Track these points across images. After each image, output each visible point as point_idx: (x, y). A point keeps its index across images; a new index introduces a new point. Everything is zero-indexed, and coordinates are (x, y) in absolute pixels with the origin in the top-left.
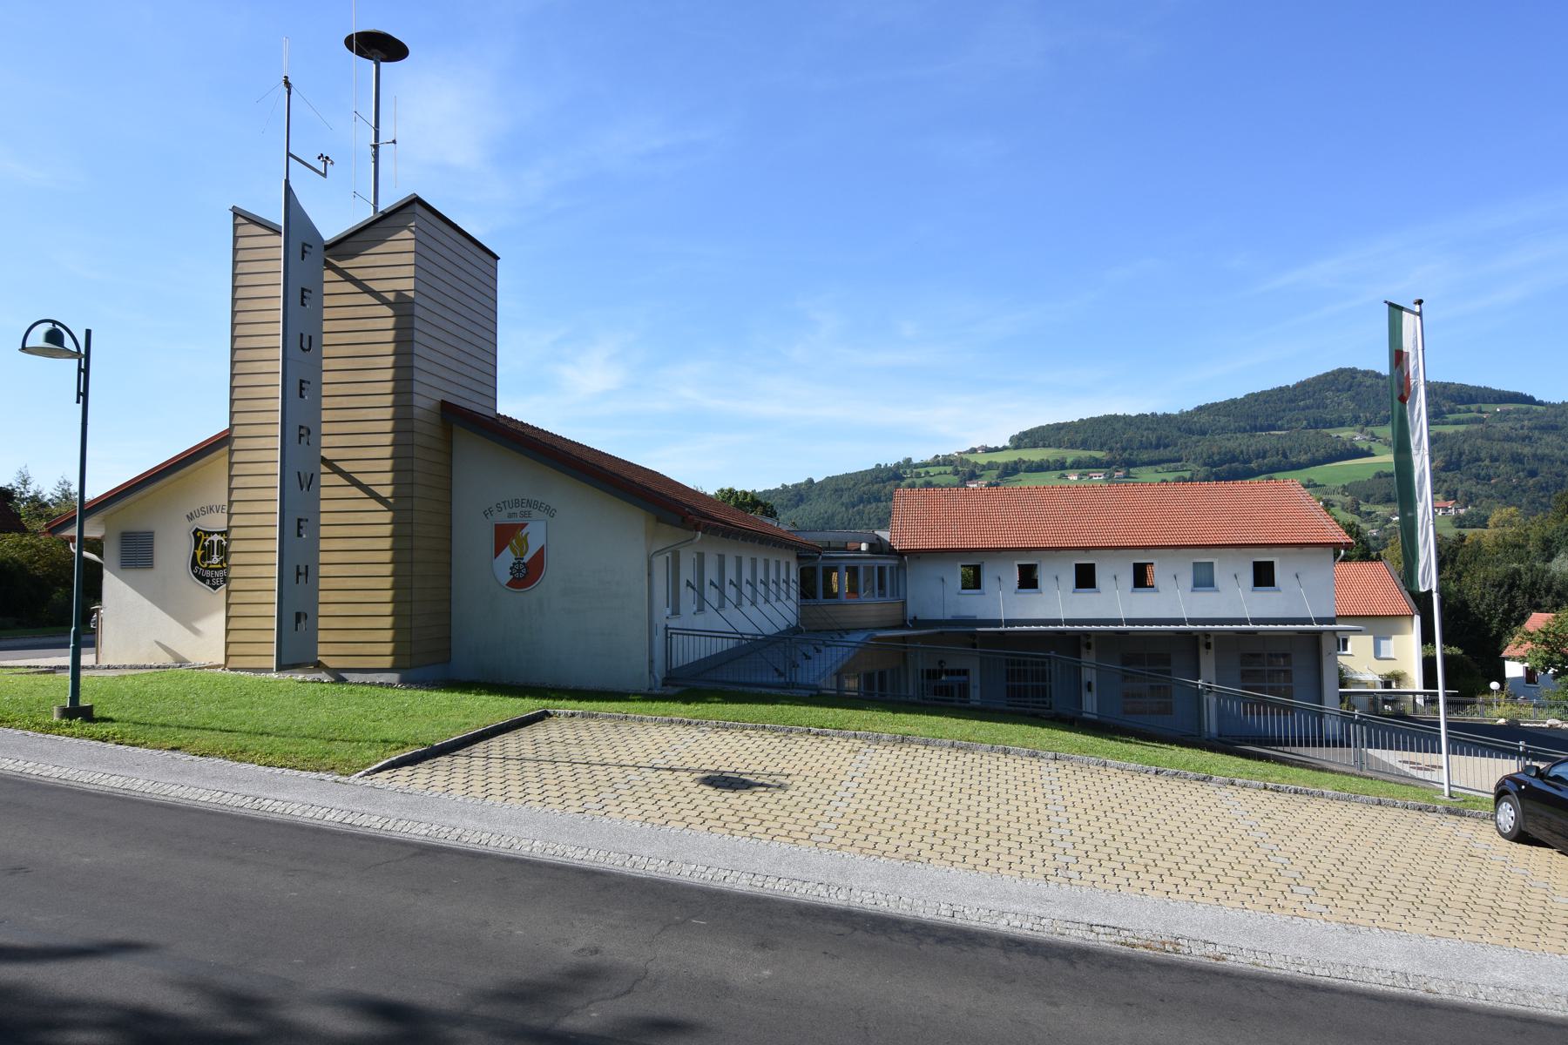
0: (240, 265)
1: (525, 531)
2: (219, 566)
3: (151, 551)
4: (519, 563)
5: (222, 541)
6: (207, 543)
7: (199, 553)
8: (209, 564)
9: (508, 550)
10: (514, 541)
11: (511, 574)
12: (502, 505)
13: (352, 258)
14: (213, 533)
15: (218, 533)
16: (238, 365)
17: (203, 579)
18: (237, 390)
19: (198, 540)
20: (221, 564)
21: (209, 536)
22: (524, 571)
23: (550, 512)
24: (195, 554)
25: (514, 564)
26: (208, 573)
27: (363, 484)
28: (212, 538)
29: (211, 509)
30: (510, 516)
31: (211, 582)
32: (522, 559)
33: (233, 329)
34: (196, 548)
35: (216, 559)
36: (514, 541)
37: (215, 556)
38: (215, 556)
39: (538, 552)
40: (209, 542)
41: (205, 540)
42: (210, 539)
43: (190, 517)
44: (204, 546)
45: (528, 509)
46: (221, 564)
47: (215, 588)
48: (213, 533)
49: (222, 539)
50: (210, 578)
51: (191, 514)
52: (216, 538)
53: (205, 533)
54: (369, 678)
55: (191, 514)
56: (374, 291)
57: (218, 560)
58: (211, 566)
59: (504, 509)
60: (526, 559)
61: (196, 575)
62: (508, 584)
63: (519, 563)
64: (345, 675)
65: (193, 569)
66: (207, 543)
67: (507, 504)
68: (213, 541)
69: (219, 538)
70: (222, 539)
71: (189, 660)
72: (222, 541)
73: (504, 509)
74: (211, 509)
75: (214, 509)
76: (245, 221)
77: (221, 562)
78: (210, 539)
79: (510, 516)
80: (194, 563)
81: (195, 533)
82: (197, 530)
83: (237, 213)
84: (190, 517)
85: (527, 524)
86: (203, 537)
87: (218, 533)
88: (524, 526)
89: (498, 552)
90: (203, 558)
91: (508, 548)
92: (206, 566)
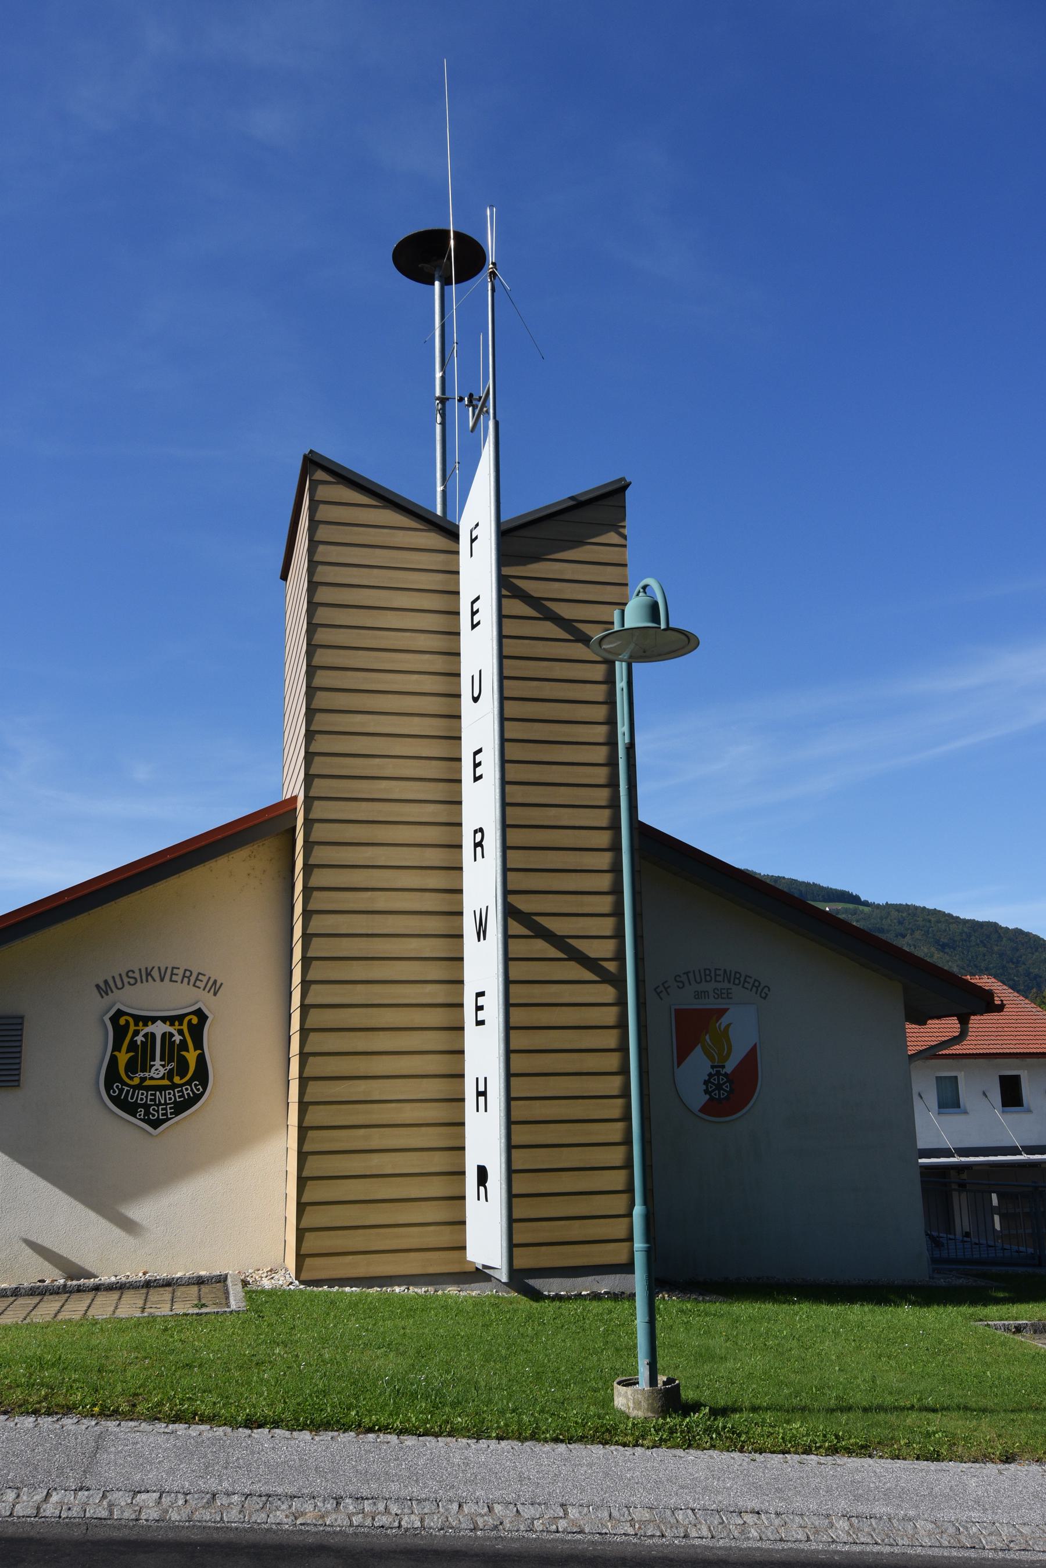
0: (321, 548)
1: (724, 1021)
2: (166, 1082)
3: (15, 1055)
4: (718, 1073)
5: (171, 1035)
6: (139, 1039)
7: (123, 1058)
8: (143, 1079)
9: (697, 1054)
10: (707, 1037)
11: (706, 1092)
12: (684, 978)
13: (524, 565)
14: (154, 1020)
15: (164, 1019)
16: (319, 717)
17: (130, 1108)
18: (317, 759)
19: (120, 1033)
20: (170, 1078)
21: (145, 1025)
22: (727, 1087)
23: (761, 990)
24: (113, 1060)
25: (710, 1075)
26: (141, 1096)
27: (556, 935)
28: (151, 1028)
29: (148, 974)
30: (698, 995)
31: (147, 1113)
32: (723, 1067)
33: (310, 654)
34: (117, 1047)
35: (158, 1069)
36: (707, 1037)
37: (158, 1063)
38: (158, 1063)
39: (747, 1055)
40: (145, 1036)
41: (136, 1033)
42: (147, 1030)
43: (104, 989)
44: (133, 1045)
45: (726, 985)
46: (170, 1078)
47: (156, 1124)
48: (154, 1020)
49: (171, 1029)
50: (146, 1107)
51: (106, 982)
52: (159, 1029)
53: (137, 1019)
54: (585, 1285)
55: (106, 982)
56: (563, 619)
57: (162, 1071)
58: (148, 1083)
59: (687, 983)
60: (729, 1067)
61: (115, 1100)
62: (703, 1110)
63: (718, 1073)
64: (535, 1283)
65: (108, 1087)
66: (139, 1039)
67: (691, 975)
68: (153, 1035)
69: (167, 1028)
70: (171, 1029)
71: (93, 1270)
72: (171, 1035)
73: (687, 983)
74: (148, 974)
75: (155, 974)
76: (328, 478)
77: (170, 1075)
78: (147, 1030)
79: (698, 995)
80: (112, 1076)
81: (115, 1019)
82: (120, 1013)
83: (312, 463)
84: (104, 989)
85: (727, 1010)
86: (132, 1028)
87: (164, 1019)
88: (722, 1012)
89: (682, 1058)
90: (131, 1067)
91: (698, 1049)
92: (136, 1081)
